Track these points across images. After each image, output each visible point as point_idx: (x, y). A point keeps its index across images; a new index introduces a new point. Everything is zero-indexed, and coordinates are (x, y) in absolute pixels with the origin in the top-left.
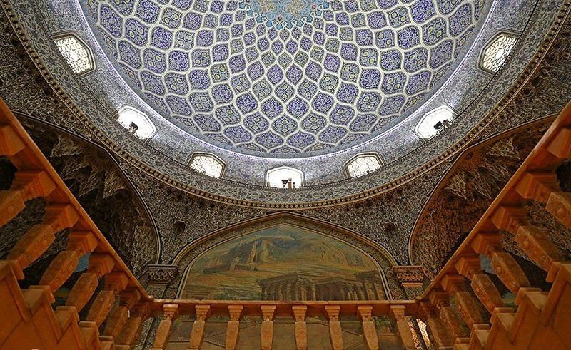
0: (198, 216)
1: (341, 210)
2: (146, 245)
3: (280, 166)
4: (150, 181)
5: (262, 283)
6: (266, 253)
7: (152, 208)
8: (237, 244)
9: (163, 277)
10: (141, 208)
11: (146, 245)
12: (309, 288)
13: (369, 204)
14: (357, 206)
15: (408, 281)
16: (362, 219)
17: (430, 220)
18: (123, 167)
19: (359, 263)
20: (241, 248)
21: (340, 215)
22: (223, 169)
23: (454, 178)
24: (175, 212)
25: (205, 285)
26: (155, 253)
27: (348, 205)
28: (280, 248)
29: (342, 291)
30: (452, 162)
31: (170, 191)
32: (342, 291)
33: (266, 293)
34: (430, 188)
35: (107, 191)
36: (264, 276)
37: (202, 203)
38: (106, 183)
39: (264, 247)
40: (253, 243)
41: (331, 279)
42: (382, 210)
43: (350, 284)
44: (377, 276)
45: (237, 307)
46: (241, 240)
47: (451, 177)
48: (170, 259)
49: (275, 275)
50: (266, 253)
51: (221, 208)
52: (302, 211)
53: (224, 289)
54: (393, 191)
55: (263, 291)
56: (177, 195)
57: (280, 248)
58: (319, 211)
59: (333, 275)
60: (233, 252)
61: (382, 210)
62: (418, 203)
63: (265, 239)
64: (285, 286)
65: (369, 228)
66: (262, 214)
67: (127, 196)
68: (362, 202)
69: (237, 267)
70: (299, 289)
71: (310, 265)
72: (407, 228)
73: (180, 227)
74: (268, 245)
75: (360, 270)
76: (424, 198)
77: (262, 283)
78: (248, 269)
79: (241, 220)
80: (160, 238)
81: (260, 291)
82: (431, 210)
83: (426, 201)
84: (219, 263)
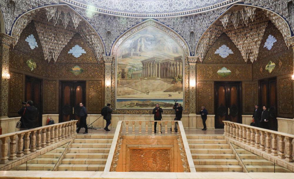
0: (115, 25)
1: (174, 19)
2: (99, 45)
12: (158, 65)
15: (192, 62)
16: (182, 25)
17: (209, 33)
18: (77, 11)
21: (174, 22)
23: (225, 16)
25: (124, 63)
26: (103, 48)
29: (169, 66)
30: (227, 8)
32: (169, 66)
33: (144, 67)
34: (213, 18)
36: (143, 59)
38: (73, 21)
40: (138, 40)
41: (166, 60)
42: (192, 21)
43: (172, 62)
44: (182, 59)
47: (224, 15)
48: (109, 51)
49: (147, 58)
51: (123, 19)
52: (158, 18)
53: (131, 65)
54: (198, 14)
55: (143, 66)
59: (167, 58)
61: (192, 21)
62: (206, 24)
63: (143, 37)
64: (150, 64)
65: (184, 31)
66: (140, 20)
67: (83, 23)
70: (155, 65)
73: (109, 33)
75: (177, 55)
76: (209, 24)
78: (137, 55)
80: (103, 42)
81: (142, 66)
82: (211, 28)
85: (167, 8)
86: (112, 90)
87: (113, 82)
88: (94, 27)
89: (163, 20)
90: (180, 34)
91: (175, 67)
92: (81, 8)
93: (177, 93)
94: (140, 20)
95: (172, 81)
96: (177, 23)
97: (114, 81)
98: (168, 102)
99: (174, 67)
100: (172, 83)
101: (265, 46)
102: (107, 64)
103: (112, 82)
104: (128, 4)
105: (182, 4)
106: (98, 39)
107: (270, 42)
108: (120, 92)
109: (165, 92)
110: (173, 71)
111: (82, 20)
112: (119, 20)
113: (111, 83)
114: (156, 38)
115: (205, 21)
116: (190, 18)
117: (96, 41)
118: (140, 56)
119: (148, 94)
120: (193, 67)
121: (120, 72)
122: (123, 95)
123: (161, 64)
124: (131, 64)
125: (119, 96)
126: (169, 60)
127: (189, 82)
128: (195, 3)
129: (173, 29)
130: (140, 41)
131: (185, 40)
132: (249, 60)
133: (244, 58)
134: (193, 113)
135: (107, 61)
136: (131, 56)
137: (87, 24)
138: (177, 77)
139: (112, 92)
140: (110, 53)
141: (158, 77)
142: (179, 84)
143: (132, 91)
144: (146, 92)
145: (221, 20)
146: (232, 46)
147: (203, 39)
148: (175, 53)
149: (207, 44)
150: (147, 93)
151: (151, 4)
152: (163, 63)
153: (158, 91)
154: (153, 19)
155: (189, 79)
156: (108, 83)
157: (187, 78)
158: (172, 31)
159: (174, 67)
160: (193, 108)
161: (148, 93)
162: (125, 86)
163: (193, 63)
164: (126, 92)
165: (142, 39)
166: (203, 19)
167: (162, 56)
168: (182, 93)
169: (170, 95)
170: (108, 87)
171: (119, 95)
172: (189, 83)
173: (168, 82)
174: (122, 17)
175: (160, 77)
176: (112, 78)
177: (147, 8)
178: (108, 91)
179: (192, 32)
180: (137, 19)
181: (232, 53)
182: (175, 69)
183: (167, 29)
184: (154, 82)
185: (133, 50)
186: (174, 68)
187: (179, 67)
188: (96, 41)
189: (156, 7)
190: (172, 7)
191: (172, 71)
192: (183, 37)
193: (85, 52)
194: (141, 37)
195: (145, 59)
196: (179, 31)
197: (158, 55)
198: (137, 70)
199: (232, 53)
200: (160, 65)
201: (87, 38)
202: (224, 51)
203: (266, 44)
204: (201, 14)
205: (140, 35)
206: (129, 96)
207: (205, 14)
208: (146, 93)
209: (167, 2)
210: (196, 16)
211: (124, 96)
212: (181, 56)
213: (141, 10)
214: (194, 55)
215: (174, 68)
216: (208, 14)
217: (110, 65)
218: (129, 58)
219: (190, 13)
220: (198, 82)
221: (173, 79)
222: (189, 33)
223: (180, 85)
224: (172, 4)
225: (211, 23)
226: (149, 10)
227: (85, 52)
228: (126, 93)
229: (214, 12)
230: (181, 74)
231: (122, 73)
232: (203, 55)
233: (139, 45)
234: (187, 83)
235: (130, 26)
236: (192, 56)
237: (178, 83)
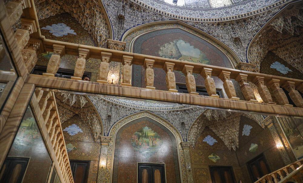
35: (82, 104)
45: (106, 90)
101: (243, 135)
103: (107, 163)
107: (247, 130)
111: (89, 101)
113: (107, 164)
132: (232, 148)
133: (228, 146)
145: (204, 114)
146: (215, 136)
154: (149, 110)
176: (107, 159)
181: (217, 142)
199: (217, 142)
202: (210, 141)
203: (243, 132)
226: (144, 105)
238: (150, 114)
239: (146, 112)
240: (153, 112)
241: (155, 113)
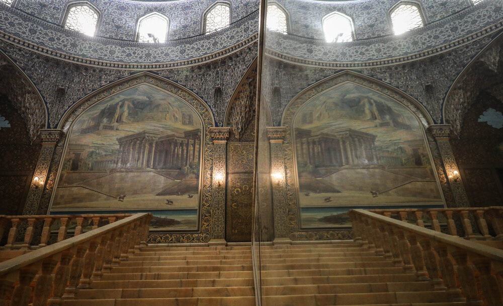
0: (76, 80)
2: (37, 111)
3: (151, 11)
4: (26, 53)
5: (120, 141)
6: (126, 114)
7: (34, 79)
8: (106, 105)
9: (52, 139)
10: (25, 79)
11: (37, 111)
12: (151, 145)
13: (208, 66)
14: (199, 67)
15: (218, 139)
16: (202, 80)
17: (247, 87)
19: (191, 123)
20: (109, 109)
22: (99, 18)
24: (55, 77)
27: (192, 67)
28: (140, 109)
29: (172, 147)
31: (47, 59)
32: (172, 147)
36: (122, 134)
37: (77, 67)
39: (126, 108)
40: (117, 104)
41: (168, 136)
44: (199, 134)
46: (110, 100)
49: (131, 133)
50: (126, 114)
52: (157, 71)
53: (95, 146)
54: (225, 58)
55: (120, 148)
56: (55, 63)
57: (140, 109)
58: (171, 71)
59: (170, 133)
60: (103, 113)
61: (217, 73)
63: (127, 100)
65: (205, 89)
66: (126, 74)
68: (204, 65)
69: (105, 128)
71: (156, 125)
72: (230, 91)
73: (61, 93)
74: (129, 107)
75: (189, 128)
77: (120, 141)
78: (111, 128)
79: (110, 82)
80: (46, 105)
81: (118, 147)
83: (245, 71)
84: (92, 123)
85: (177, 56)
86: (44, 193)
87: (50, 178)
88: (31, 78)
89: (167, 73)
90: (197, 94)
91: (185, 148)
92: (7, 42)
93: (186, 196)
94: (126, 74)
95: (176, 173)
96: (193, 77)
97: (55, 175)
98: (163, 217)
99: (182, 148)
100: (176, 177)
102: (46, 145)
104: (106, 50)
105: (201, 48)
106: (39, 101)
108: (62, 197)
109: (158, 195)
110: (180, 156)
112: (85, 72)
114: (151, 102)
115: (238, 68)
116: (215, 68)
117: (32, 104)
118: (117, 129)
119: (122, 200)
120: (220, 148)
121: (70, 159)
122: (66, 203)
123: (156, 143)
124: (96, 145)
125: (58, 206)
126: (173, 135)
127: (211, 175)
128: (221, 44)
129: (185, 86)
130: (121, 106)
131: (206, 102)
134: (218, 237)
135: (48, 139)
136: (98, 129)
137: (18, 73)
138: (188, 166)
139: (42, 197)
140: (57, 125)
141: (148, 166)
142: (190, 180)
143: (88, 194)
144: (117, 196)
147: (239, 98)
148: (186, 124)
149: (246, 107)
150: (120, 198)
151: (149, 51)
152: (162, 142)
153: (145, 193)
154: (150, 71)
155: (212, 169)
156: (39, 179)
157: (210, 166)
158: (183, 90)
159: (182, 148)
160: (218, 226)
161: (123, 199)
162: (75, 185)
163: (221, 139)
164: (75, 196)
165: (126, 102)
166: (236, 65)
167: (161, 130)
168: (196, 197)
169: (170, 202)
170: (37, 187)
171: (59, 204)
172: (212, 178)
173: (168, 175)
174: (92, 67)
175: (152, 167)
177: (141, 58)
178: (34, 195)
179: (219, 89)
180: (120, 72)
182: (185, 151)
183: (176, 87)
184: (138, 176)
185: (105, 120)
186: (183, 150)
187: (192, 148)
188: (32, 104)
189: (157, 56)
190: (185, 54)
191: (178, 155)
192: (202, 98)
193: (9, 126)
194: (123, 101)
195: (126, 135)
196: (195, 89)
197: (153, 128)
198: (106, 155)
200: (154, 145)
201: (17, 100)
204: (230, 58)
205: (122, 97)
206: (82, 204)
207: (237, 56)
208: (118, 198)
209: (177, 48)
210: (223, 62)
211: (68, 205)
212: (198, 130)
213: (130, 60)
214: (222, 126)
215: (183, 150)
216: (241, 54)
217: (53, 146)
218: (92, 134)
219: (213, 58)
220: (230, 177)
221: (178, 170)
222: (214, 90)
223: (194, 182)
224: (185, 51)
225: (247, 68)
227: (9, 126)
228: (74, 199)
229: (250, 49)
230: (196, 160)
231: (74, 161)
232: (240, 126)
233: (118, 113)
234: (209, 176)
235: (106, 82)
236: (221, 128)
237: (188, 178)
238: (153, 78)
239: (146, 76)
240: (158, 74)
241: (160, 76)
